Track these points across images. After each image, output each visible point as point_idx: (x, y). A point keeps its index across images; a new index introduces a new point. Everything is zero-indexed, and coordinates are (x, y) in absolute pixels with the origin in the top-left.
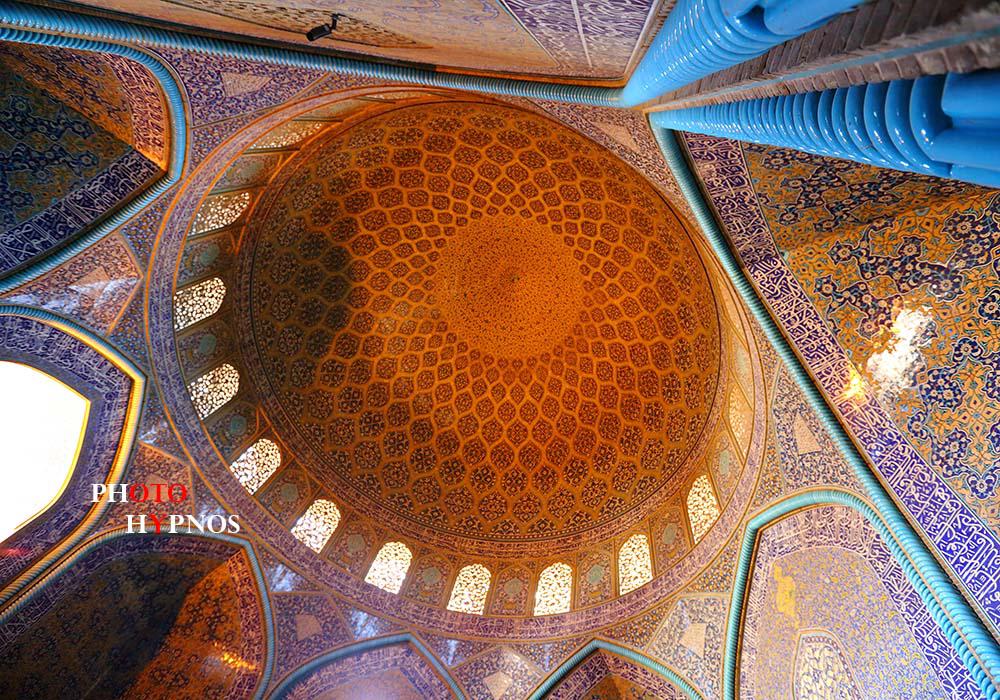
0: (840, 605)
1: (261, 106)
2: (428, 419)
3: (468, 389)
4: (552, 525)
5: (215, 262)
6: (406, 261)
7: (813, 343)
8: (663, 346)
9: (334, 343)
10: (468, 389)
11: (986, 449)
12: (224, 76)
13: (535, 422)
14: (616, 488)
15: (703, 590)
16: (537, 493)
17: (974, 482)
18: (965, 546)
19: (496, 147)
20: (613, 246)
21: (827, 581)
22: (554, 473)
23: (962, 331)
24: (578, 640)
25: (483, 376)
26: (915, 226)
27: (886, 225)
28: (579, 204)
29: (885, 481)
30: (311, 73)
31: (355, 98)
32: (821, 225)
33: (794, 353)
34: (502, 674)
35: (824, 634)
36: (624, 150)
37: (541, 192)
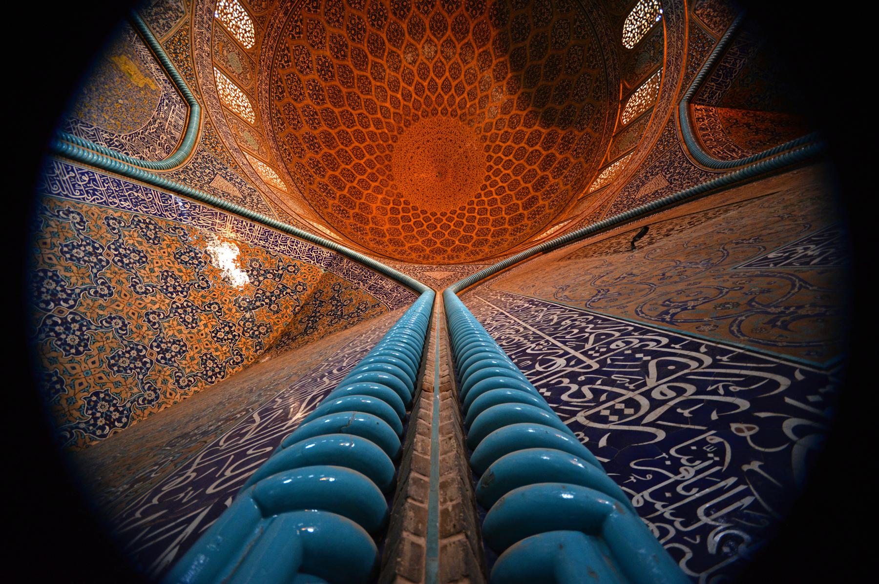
1: (634, 181)
2: (439, 39)
3: (425, 84)
4: (309, 10)
5: (636, 60)
6: (504, 145)
8: (341, 188)
9: (528, 55)
10: (425, 84)
12: (667, 184)
13: (373, 89)
16: (336, 31)
19: (487, 234)
20: (402, 224)
25: (422, 100)
28: (431, 233)
29: (160, 191)
30: (612, 214)
31: (578, 216)
36: (431, 270)
37: (452, 227)
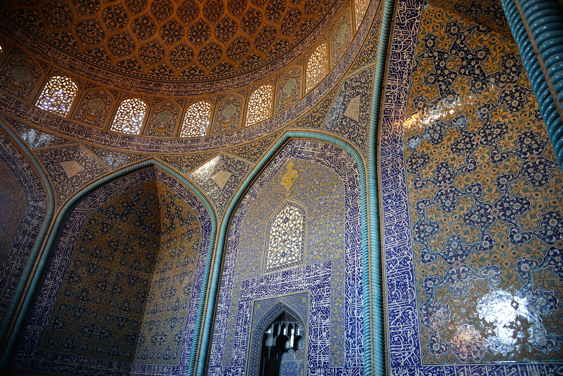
0: (317, 196)
7: (399, 67)
11: (432, 170)
14: (200, 60)
15: (239, 155)
16: (134, 36)
17: (417, 181)
18: (395, 204)
21: (317, 183)
22: (153, 25)
23: (465, 112)
24: (140, 156)
26: (494, 44)
27: (484, 32)
29: (379, 157)
32: (459, 6)
33: (384, 66)
34: (76, 163)
35: (300, 205)
